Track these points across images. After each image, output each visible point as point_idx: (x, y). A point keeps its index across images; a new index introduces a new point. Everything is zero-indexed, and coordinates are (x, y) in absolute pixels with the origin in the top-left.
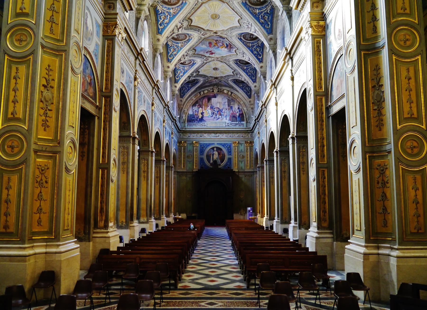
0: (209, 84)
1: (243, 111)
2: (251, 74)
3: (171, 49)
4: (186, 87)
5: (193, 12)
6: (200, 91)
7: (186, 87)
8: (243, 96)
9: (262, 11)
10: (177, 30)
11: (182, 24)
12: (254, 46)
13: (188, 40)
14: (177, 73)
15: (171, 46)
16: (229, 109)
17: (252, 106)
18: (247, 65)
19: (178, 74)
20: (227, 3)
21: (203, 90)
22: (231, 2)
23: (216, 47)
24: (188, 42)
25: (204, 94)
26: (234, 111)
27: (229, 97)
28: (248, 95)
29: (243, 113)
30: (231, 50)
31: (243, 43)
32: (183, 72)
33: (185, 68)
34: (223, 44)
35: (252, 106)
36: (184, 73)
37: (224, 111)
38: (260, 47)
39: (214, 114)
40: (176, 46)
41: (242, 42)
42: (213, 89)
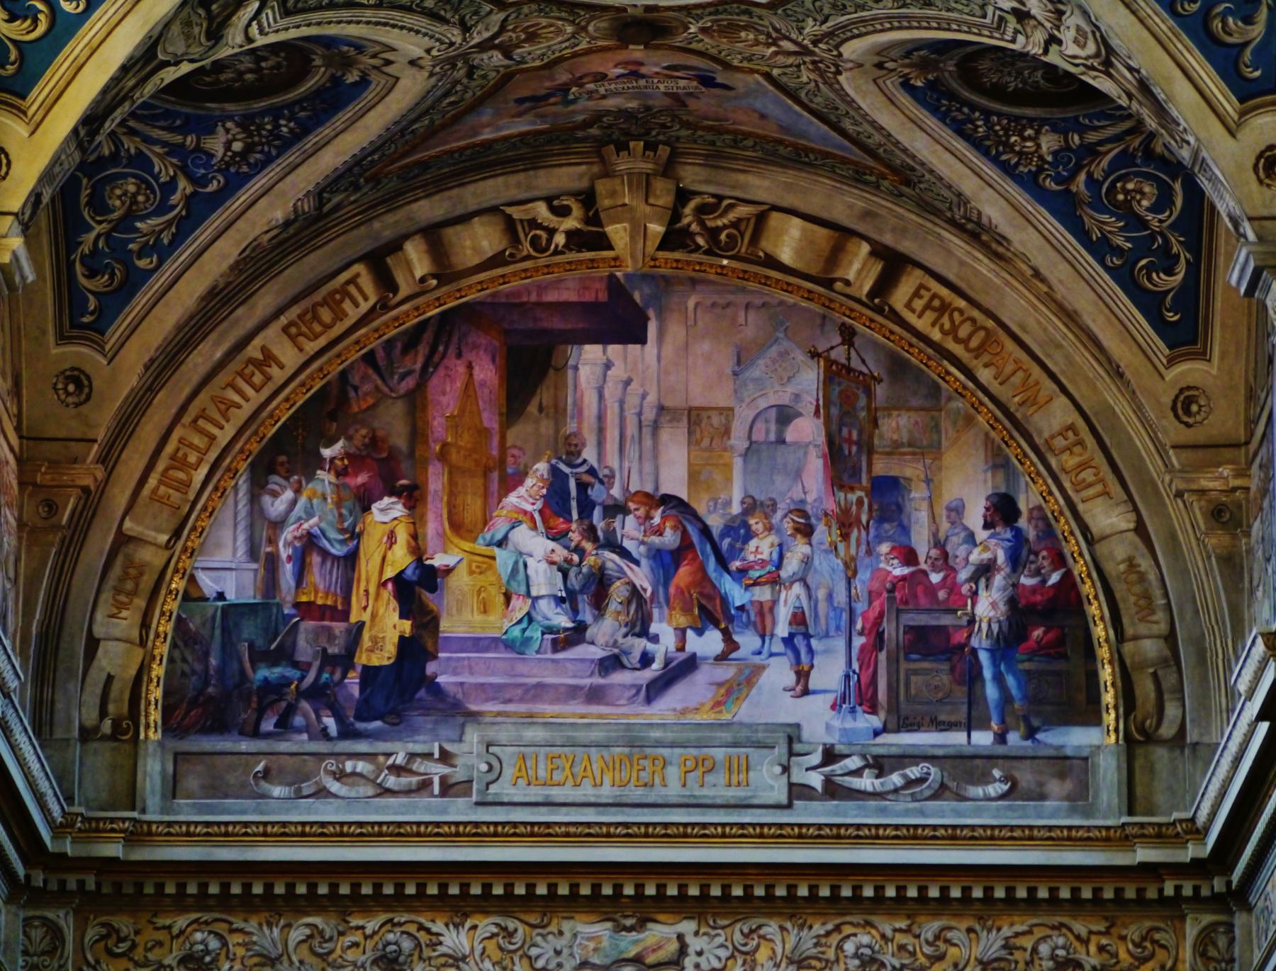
0: (522, 126)
1: (1073, 546)
4: (164, 169)
6: (385, 226)
7: (164, 169)
8: (1070, 316)
16: (845, 523)
17: (1218, 479)
21: (428, 209)
25: (445, 273)
26: (921, 543)
27: (848, 335)
28: (1150, 304)
29: (1068, 581)
35: (1218, 479)
37: (761, 547)
39: (599, 602)
42: (588, 198)
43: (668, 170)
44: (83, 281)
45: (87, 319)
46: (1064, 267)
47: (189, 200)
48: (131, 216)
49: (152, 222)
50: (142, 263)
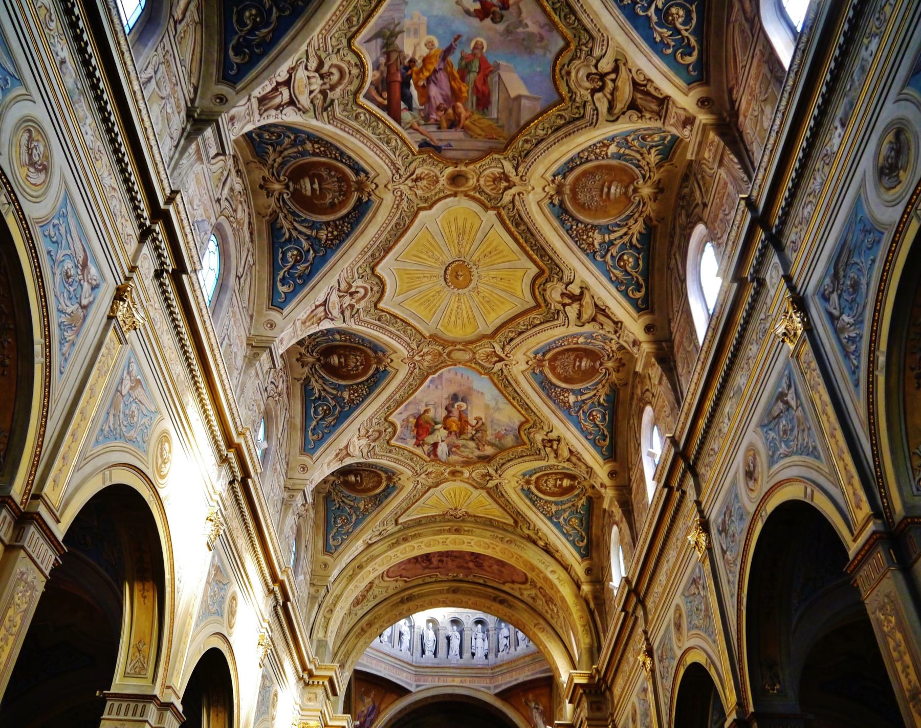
5: (521, 321)
11: (564, 305)
12: (293, 144)
13: (572, 169)
15: (652, 147)
20: (425, 338)
22: (414, 346)
23: (454, 59)
24: (572, 160)
30: (383, 60)
31: (342, 153)
34: (424, 91)
38: (267, 144)
40: (629, 148)
41: (350, 158)
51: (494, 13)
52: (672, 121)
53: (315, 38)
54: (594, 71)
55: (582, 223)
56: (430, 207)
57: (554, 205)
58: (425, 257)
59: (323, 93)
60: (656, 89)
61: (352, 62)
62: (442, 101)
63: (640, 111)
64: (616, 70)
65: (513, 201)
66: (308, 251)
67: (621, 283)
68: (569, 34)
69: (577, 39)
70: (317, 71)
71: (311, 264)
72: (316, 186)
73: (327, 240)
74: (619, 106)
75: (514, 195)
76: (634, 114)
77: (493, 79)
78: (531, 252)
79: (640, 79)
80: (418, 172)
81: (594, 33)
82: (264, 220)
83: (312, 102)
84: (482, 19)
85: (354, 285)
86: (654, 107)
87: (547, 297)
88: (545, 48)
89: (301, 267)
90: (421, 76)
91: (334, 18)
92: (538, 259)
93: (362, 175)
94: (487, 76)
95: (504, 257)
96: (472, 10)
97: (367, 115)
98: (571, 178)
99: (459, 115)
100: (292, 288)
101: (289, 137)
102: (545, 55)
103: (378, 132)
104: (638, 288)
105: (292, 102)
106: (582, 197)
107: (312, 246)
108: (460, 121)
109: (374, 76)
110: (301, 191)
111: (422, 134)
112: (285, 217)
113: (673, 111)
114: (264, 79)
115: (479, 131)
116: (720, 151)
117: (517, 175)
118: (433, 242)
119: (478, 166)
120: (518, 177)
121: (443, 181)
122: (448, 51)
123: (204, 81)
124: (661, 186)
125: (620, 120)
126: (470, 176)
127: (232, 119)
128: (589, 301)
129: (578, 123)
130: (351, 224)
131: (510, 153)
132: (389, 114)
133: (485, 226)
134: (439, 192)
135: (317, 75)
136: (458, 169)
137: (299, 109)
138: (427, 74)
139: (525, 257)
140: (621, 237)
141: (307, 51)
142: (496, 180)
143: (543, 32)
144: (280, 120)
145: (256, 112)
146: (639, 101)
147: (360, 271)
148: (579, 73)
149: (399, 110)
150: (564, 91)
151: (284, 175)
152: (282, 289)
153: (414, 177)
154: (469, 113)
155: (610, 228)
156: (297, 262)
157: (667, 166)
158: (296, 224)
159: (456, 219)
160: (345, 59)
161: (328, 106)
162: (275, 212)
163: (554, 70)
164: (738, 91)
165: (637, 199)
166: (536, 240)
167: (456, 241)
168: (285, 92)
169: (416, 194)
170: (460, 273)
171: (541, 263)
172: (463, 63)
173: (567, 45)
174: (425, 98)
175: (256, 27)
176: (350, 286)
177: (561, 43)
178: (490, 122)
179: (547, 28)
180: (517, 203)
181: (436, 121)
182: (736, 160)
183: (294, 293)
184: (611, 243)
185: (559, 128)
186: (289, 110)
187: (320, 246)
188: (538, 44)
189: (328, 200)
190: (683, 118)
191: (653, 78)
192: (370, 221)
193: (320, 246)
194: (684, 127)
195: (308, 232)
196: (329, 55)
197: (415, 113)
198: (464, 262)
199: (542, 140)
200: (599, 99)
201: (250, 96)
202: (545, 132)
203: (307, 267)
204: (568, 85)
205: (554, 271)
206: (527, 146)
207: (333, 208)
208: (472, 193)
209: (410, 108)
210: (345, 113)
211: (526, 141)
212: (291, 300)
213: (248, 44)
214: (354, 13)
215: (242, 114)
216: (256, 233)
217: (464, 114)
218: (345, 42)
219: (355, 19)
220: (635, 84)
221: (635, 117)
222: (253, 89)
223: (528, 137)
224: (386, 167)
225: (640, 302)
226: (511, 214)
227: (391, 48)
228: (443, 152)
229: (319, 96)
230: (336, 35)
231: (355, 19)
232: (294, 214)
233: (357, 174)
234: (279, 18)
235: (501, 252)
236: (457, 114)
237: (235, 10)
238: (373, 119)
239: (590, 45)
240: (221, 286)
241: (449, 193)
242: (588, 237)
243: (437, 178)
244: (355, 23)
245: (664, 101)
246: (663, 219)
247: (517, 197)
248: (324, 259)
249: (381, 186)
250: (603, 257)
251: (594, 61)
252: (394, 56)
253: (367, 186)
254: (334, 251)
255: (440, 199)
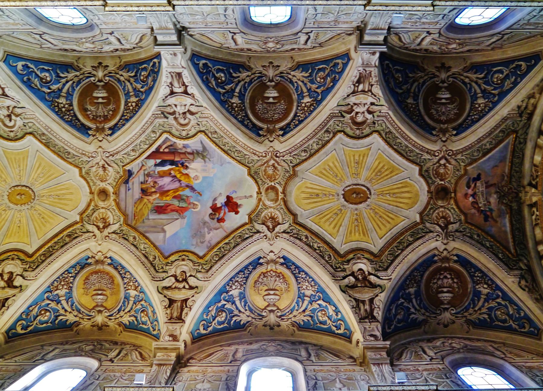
2: (328, 75)
3: (143, 319)
4: (493, 304)
6: (533, 254)
7: (493, 304)
9: (305, 90)
10: (7, 290)
12: (135, 89)
13: (116, 268)
14: (324, 323)
15: (136, 317)
18: (295, 97)
19: (329, 322)
21: (531, 244)
24: (123, 268)
28: (530, 69)
30: (189, 150)
31: (127, 120)
32: (324, 304)
33: (308, 293)
34: (168, 174)
36: (328, 300)
38: (136, 72)
41: (124, 125)
42: (531, 206)
43: (524, 187)
44: (526, 330)
45: (536, 332)
46: (522, 91)
47: (503, 299)
48: (508, 314)
49: (510, 310)
50: (522, 314)
51: (215, 214)
52: (170, 328)
53: (209, 112)
54: (188, 275)
55: (74, 280)
56: (82, 176)
57: (87, 260)
58: (39, 172)
59: (174, 113)
60: (187, 314)
61: (190, 132)
62: (160, 185)
63: (169, 306)
64: (191, 288)
65: (88, 232)
66: (50, 89)
67: (28, 315)
68: (207, 258)
69: (205, 263)
70: (189, 111)
71: (39, 89)
72: (100, 100)
73: (58, 103)
74: (169, 293)
75: (93, 232)
76: (167, 303)
77: (175, 215)
78: (46, 247)
79: (189, 303)
80: (110, 169)
81: (210, 272)
82: (74, 61)
83: (169, 105)
84: (211, 207)
85: (18, 119)
86: (175, 315)
87: (6, 261)
88: (197, 245)
89: (36, 81)
90: (178, 172)
91: (218, 124)
92: (41, 252)
93: (110, 132)
94: (177, 211)
95: (40, 227)
96: (216, 202)
97: (154, 139)
98: (110, 269)
99: (150, 195)
100: (20, 72)
101: (142, 88)
102: (192, 245)
103: (142, 144)
104: (24, 328)
105: (172, 93)
106: (95, 277)
107: (54, 92)
108: (146, 196)
109: (180, 144)
110: (96, 90)
111: (138, 172)
112: (76, 76)
113: (177, 326)
114: (191, 79)
115: (139, 208)
116: (167, 362)
117: (109, 233)
118: (53, 177)
119: (114, 208)
120: (107, 234)
121: (103, 185)
122: (192, 189)
123: (193, 42)
124: (104, 328)
125: (160, 295)
126: (106, 203)
127: (175, 54)
128: (10, 294)
129: (152, 269)
130: (71, 121)
131: (125, 228)
132: (153, 152)
133: (66, 214)
134: (93, 182)
135: (186, 110)
136: (112, 194)
137: (166, 97)
138: (178, 176)
139: (42, 243)
140: (63, 308)
141: (202, 106)
142: (104, 220)
143: (206, 243)
144: (163, 84)
145: (173, 70)
146: (176, 305)
147: (30, 124)
148: (186, 266)
149: (155, 159)
150: (172, 258)
151: (109, 80)
152: (20, 65)
153: (106, 166)
154: (152, 201)
155: (70, 300)
156: (41, 79)
157: (120, 329)
158: (71, 82)
159: (71, 193)
160: (193, 128)
161: (164, 115)
162: (81, 69)
163: (184, 251)
164: (196, 363)
165: (93, 314)
166: (57, 250)
167: (52, 193)
168: (182, 90)
169: (92, 167)
170: (23, 197)
171: (37, 255)
172: (184, 197)
173: (201, 258)
174: (162, 175)
175: (216, 79)
176: (17, 116)
177: (201, 254)
178: (146, 215)
179: (209, 245)
180: (88, 234)
181: (147, 181)
182: (168, 374)
183: (16, 73)
184: (58, 302)
185: (147, 258)
186: (168, 91)
187: (53, 98)
188: (199, 241)
189: (89, 107)
190: (175, 334)
191: (192, 310)
192: (73, 134)
193: (53, 98)
194: (170, 336)
195: (65, 90)
196: (197, 119)
197: (153, 168)
198: (34, 199)
199: (137, 248)
200: (170, 280)
201: (185, 68)
202: (143, 249)
203: (36, 86)
204: (176, 260)
205: (32, 265)
206: (131, 239)
207: (84, 110)
208: (93, 204)
209: (156, 165)
210: (157, 125)
211: (134, 238)
212: (11, 70)
213: (208, 72)
214: (219, 135)
215: (176, 62)
216: (65, 53)
217: (151, 198)
218: (203, 129)
219: (215, 136)
220: (186, 300)
221: (165, 304)
222: (188, 71)
223: (137, 239)
224: (115, 148)
225: (14, 331)
226: (78, 231)
227: (195, 155)
228: (124, 185)
229: (172, 111)
230: (208, 124)
231: (215, 136)
232: (79, 82)
233: (110, 129)
234: (220, 93)
235: (45, 226)
236: (151, 194)
237: (225, 68)
238: (151, 142)
239: (203, 271)
240: (41, 20)
241: (93, 189)
242: (63, 285)
243: (105, 181)
244: (213, 136)
245: (180, 319)
246: (78, 334)
247: (92, 234)
248: (42, 99)
249: (100, 144)
250: (48, 298)
251: (194, 274)
252: (191, 157)
253: (100, 134)
254: (49, 107)
255: (88, 183)
